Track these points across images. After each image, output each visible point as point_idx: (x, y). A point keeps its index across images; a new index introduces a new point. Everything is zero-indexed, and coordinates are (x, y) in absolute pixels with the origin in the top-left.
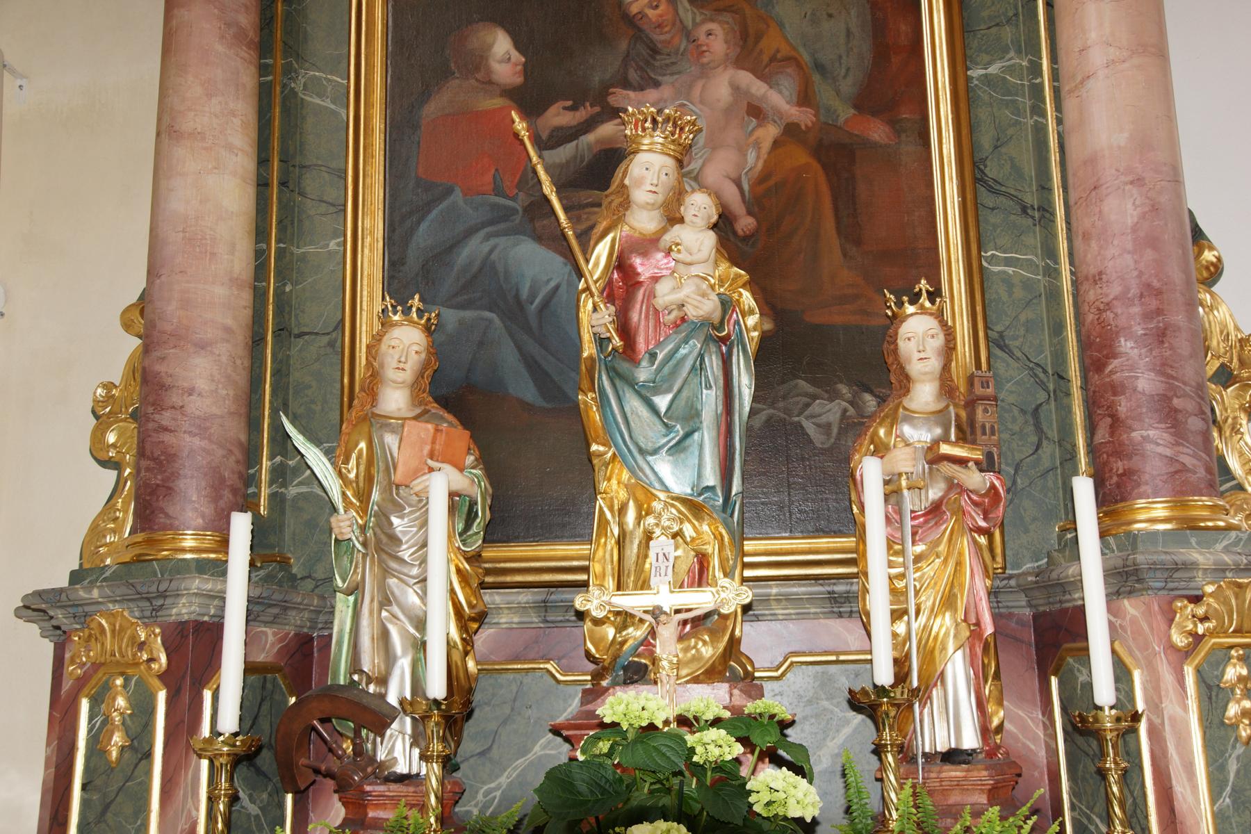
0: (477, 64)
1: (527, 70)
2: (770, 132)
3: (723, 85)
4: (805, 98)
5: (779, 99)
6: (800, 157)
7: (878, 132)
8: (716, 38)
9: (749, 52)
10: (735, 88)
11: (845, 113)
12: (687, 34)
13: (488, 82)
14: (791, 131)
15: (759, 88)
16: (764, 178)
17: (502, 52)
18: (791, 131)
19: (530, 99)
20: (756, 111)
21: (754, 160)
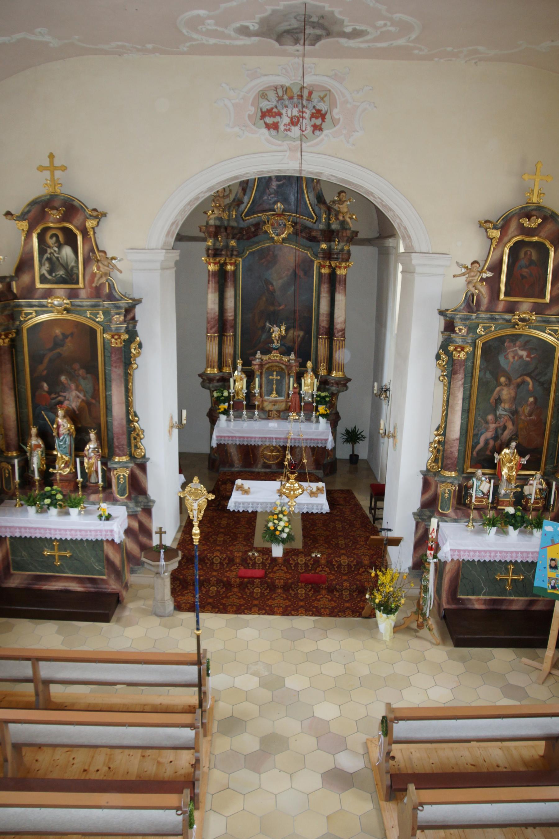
0: (42, 387)
1: (49, 389)
2: (80, 400)
3: (74, 393)
4: (85, 396)
5: (81, 396)
6: (84, 404)
7: (94, 401)
8: (73, 386)
9: (77, 389)
10: (76, 394)
11: (90, 399)
12: (69, 385)
13: (44, 390)
14: (83, 400)
15: (78, 394)
16: (79, 406)
17: (45, 385)
18: (83, 400)
19: (50, 393)
20: (78, 397)
21: (78, 404)
